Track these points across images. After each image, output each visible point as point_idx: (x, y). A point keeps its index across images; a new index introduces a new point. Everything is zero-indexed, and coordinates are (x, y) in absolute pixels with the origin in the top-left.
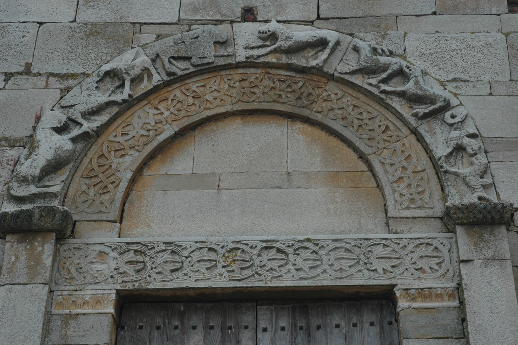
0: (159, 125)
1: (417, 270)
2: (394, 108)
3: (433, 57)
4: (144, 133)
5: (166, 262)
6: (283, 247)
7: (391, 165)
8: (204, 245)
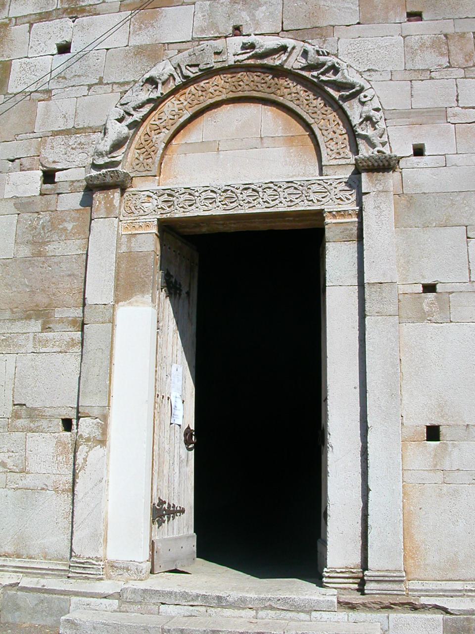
0: (181, 111)
1: (338, 199)
4: (172, 117)
5: (186, 200)
6: (255, 187)
7: (326, 130)
8: (208, 188)
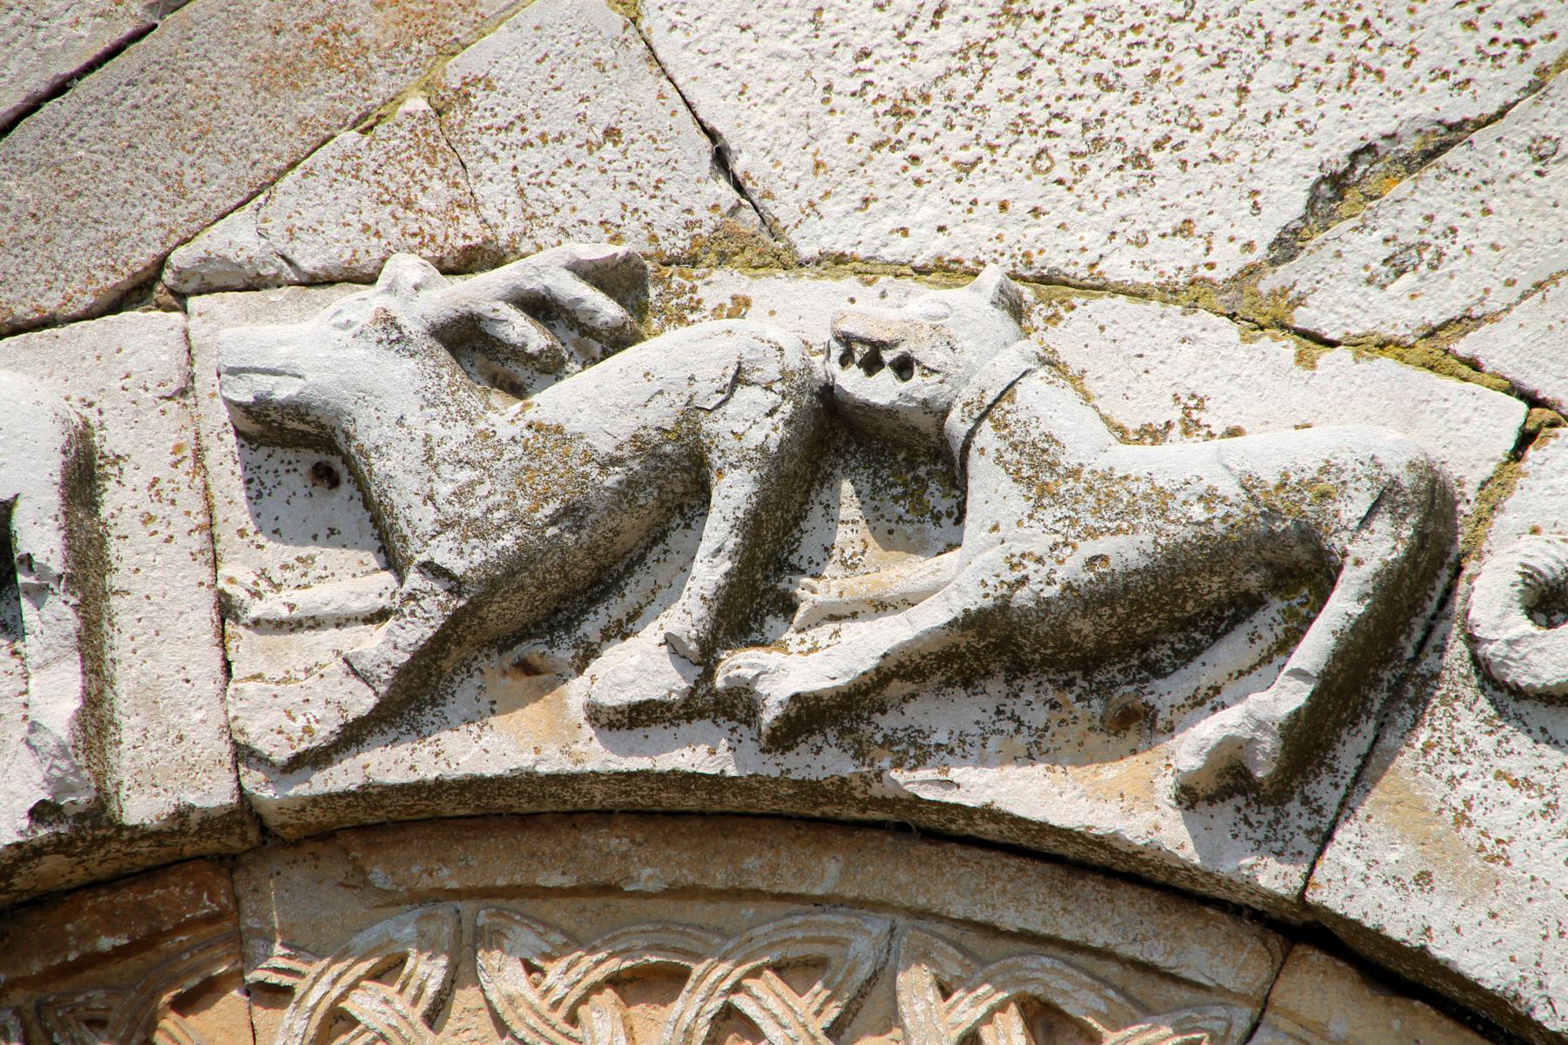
2: (991, 814)
3: (1003, 77)
